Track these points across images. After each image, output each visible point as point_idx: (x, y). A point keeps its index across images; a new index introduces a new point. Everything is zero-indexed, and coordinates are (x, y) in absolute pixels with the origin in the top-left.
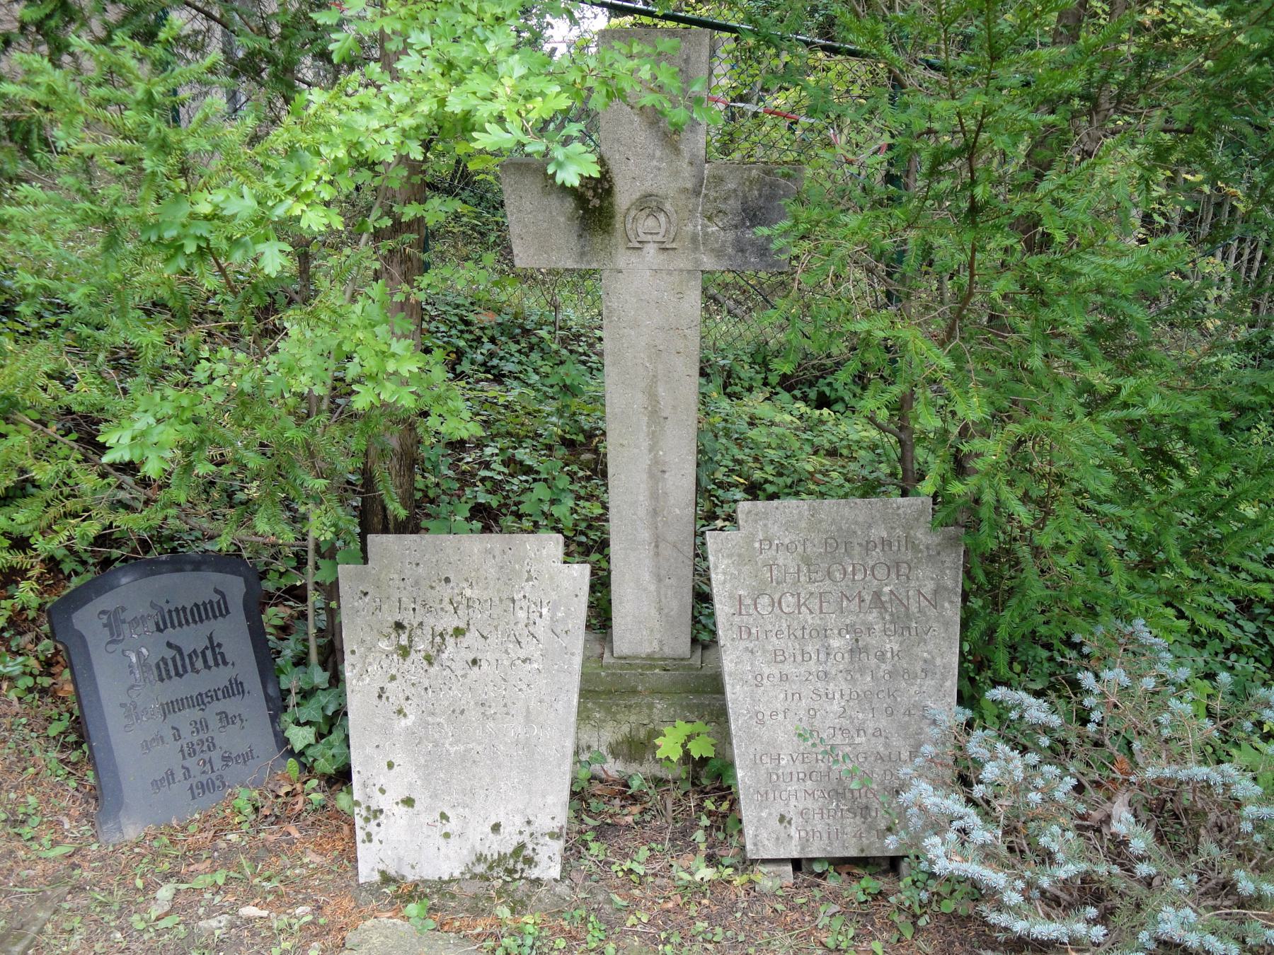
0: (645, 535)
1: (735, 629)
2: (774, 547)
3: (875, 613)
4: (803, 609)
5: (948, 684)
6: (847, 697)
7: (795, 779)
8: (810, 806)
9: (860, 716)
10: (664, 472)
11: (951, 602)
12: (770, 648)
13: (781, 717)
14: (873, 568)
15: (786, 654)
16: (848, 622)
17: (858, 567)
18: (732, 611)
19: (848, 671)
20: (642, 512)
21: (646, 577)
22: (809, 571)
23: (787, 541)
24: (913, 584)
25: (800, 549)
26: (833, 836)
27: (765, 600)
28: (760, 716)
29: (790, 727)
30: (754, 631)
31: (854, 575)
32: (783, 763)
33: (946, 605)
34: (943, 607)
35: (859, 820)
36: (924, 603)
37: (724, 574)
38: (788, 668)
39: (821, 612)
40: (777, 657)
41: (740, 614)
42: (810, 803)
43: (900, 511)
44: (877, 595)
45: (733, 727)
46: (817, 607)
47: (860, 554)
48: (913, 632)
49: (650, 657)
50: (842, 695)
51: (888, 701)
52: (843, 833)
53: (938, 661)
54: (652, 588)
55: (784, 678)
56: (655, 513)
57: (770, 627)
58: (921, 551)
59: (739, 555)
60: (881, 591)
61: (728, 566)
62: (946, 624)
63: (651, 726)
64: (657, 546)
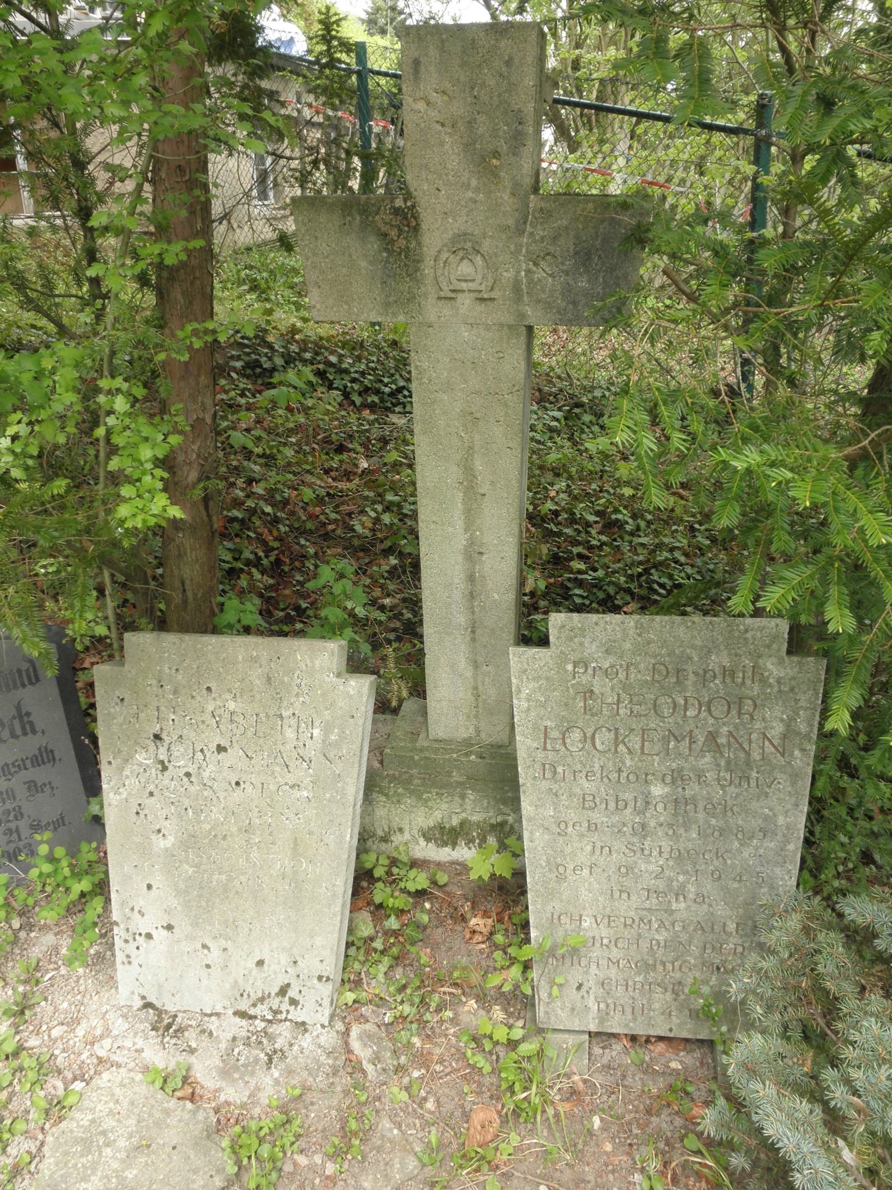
0: (461, 619)
1: (538, 766)
2: (590, 671)
3: (708, 758)
4: (621, 747)
5: (791, 847)
6: (665, 855)
7: (598, 945)
8: (613, 976)
9: (681, 878)
10: (481, 553)
11: (803, 750)
12: (578, 791)
13: (586, 871)
14: (709, 704)
15: (598, 800)
16: (674, 766)
17: (691, 701)
18: (535, 745)
19: (670, 826)
20: (457, 595)
21: (463, 664)
22: (631, 701)
23: (606, 665)
24: (758, 725)
25: (622, 676)
26: (638, 1011)
27: (576, 735)
28: (561, 869)
29: (596, 886)
30: (560, 770)
31: (686, 710)
32: (585, 925)
33: (797, 753)
34: (791, 755)
35: (669, 996)
36: (769, 749)
37: (528, 700)
38: (597, 817)
39: (643, 752)
40: (586, 802)
41: (545, 749)
42: (613, 972)
43: (749, 635)
44: (712, 737)
45: (528, 880)
46: (637, 747)
47: (695, 684)
48: (753, 783)
50: (660, 853)
51: (716, 863)
52: (650, 1009)
53: (781, 820)
54: (469, 674)
55: (593, 827)
56: (472, 596)
57: (578, 767)
58: (770, 686)
59: (547, 679)
60: (717, 732)
61: (534, 691)
62: (795, 777)
63: (464, 815)
64: (473, 632)
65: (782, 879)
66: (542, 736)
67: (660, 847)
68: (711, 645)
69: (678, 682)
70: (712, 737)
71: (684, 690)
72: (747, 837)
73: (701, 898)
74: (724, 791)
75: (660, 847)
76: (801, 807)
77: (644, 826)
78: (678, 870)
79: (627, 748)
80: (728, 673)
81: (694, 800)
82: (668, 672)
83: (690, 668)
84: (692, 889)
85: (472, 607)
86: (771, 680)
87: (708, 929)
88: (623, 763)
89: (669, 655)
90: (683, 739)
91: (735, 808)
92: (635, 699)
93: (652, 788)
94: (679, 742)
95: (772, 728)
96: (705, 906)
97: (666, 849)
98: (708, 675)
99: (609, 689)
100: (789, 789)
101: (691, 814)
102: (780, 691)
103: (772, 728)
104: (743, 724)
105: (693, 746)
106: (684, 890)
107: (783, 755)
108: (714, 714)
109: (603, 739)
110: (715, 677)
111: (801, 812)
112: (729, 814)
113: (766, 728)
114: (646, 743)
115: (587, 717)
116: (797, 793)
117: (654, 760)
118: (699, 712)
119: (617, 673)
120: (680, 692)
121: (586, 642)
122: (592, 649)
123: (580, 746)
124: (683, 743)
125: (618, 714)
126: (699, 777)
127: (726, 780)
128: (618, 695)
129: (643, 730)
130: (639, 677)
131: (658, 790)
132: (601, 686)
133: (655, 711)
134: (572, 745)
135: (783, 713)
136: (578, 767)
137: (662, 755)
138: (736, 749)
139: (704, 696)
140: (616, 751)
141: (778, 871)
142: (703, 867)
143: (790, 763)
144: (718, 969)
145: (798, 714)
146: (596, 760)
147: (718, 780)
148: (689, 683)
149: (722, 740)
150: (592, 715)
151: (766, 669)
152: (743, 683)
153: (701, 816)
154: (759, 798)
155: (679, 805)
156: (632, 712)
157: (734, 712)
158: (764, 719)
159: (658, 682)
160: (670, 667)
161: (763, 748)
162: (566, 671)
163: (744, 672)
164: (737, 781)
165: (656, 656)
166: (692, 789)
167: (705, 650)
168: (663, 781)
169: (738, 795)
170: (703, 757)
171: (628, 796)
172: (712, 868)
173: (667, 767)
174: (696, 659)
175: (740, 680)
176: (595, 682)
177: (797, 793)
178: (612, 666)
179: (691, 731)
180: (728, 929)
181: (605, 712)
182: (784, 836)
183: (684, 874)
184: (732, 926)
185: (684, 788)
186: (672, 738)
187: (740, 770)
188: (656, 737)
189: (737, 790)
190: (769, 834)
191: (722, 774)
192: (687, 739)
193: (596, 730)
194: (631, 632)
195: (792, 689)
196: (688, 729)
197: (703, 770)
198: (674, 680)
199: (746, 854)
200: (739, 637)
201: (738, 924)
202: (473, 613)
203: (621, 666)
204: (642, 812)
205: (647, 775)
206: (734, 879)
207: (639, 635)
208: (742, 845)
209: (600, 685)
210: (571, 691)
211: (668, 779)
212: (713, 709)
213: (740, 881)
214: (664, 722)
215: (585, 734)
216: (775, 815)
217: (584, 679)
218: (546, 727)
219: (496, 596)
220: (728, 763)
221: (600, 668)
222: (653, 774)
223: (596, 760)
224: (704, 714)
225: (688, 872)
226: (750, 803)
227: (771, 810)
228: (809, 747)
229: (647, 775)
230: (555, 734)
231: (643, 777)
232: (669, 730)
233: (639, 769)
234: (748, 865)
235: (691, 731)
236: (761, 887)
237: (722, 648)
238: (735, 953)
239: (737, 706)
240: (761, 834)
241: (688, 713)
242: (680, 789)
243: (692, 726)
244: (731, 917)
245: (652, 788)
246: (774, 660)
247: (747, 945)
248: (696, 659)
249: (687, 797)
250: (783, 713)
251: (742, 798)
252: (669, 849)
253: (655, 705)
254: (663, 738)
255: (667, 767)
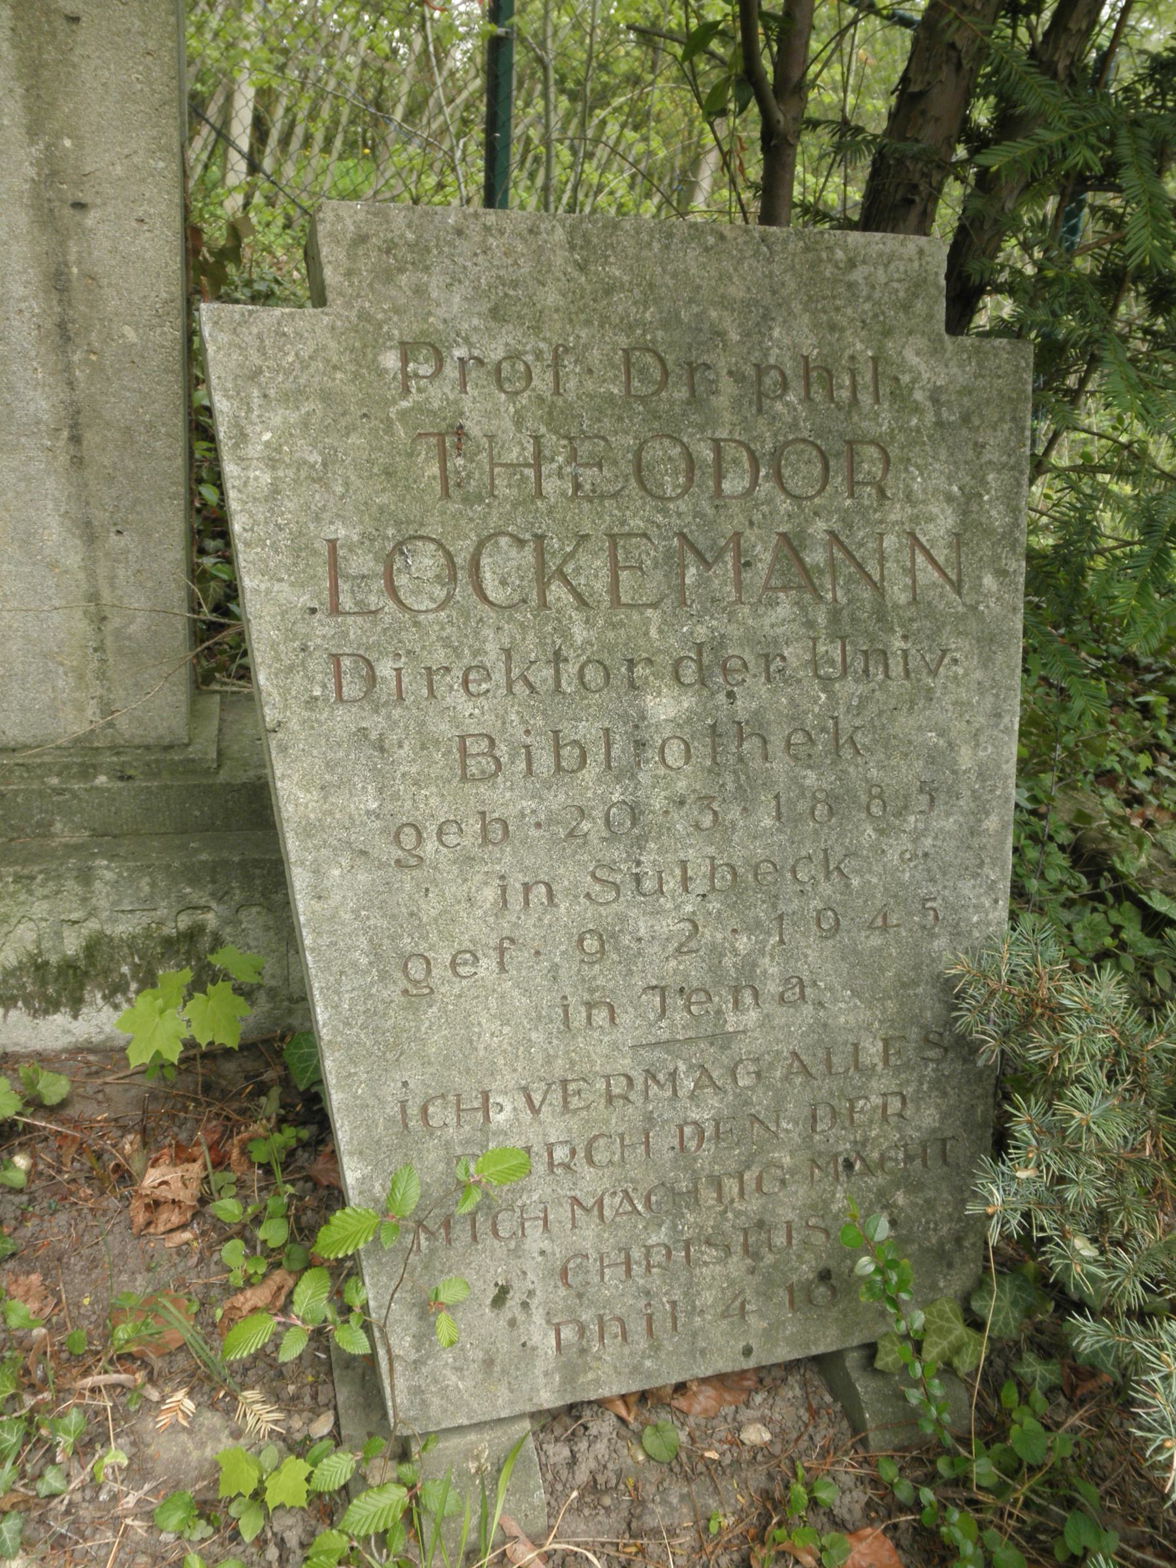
0: (40, 403)
1: (318, 665)
2: (451, 371)
3: (784, 609)
4: (557, 592)
5: (991, 823)
6: (699, 886)
7: (541, 1168)
8: (588, 1246)
9: (743, 943)
10: (79, 206)
11: (1001, 573)
12: (443, 728)
13: (487, 965)
14: (777, 455)
15: (502, 750)
16: (702, 632)
17: (730, 451)
18: (305, 600)
19: (705, 801)
20: (23, 333)
21: (54, 532)
22: (573, 457)
23: (495, 352)
24: (897, 513)
25: (542, 382)
26: (662, 1323)
27: (426, 561)
28: (416, 969)
29: (520, 1001)
30: (385, 669)
31: (719, 476)
32: (499, 1118)
33: (989, 581)
34: (977, 587)
35: (737, 1265)
36: (927, 575)
37: (272, 463)
38: (507, 798)
39: (616, 601)
40: (473, 758)
41: (335, 609)
42: (588, 1236)
43: (858, 275)
44: (791, 546)
45: (321, 1014)
46: (600, 585)
47: (737, 404)
48: (896, 669)
49: (83, 744)
50: (685, 880)
51: (825, 888)
52: (693, 1311)
53: (966, 758)
54: (73, 559)
55: (495, 831)
56: (64, 334)
57: (440, 656)
58: (917, 409)
59: (326, 396)
60: (802, 534)
61: (286, 434)
62: (988, 641)
63: (93, 925)
64: (76, 439)
65: (978, 908)
66: (323, 571)
67: (683, 864)
68: (768, 299)
69: (695, 400)
70: (791, 546)
71: (711, 421)
72: (890, 808)
73: (796, 991)
74: (831, 695)
75: (683, 864)
76: (1006, 720)
77: (635, 811)
78: (734, 923)
79: (573, 590)
80: (817, 374)
81: (757, 728)
82: (666, 373)
83: (723, 363)
84: (770, 967)
85: (68, 368)
86: (918, 395)
87: (817, 1069)
88: (566, 635)
89: (665, 325)
90: (719, 557)
91: (859, 737)
92: (584, 449)
93: (650, 701)
94: (708, 566)
95: (931, 519)
96: (808, 1009)
97: (699, 870)
98: (768, 381)
99: (508, 424)
100: (978, 675)
101: (756, 764)
102: (939, 424)
103: (931, 519)
104: (862, 511)
105: (747, 576)
106: (752, 975)
107: (958, 587)
108: (790, 485)
109: (505, 568)
110: (785, 386)
111: (1007, 731)
112: (847, 753)
113: (915, 519)
114: (624, 575)
115: (454, 507)
116: (995, 684)
117: (647, 622)
118: (755, 482)
119: (529, 378)
120: (702, 429)
121: (435, 284)
122: (452, 306)
123: (440, 593)
124: (718, 569)
125: (539, 493)
126: (767, 659)
127: (832, 663)
128: (537, 439)
129: (612, 537)
130: (590, 385)
131: (665, 706)
132: (487, 414)
133: (641, 482)
134: (416, 592)
135: (950, 479)
136: (440, 656)
137: (667, 605)
138: (850, 579)
139: (760, 438)
140: (544, 604)
141: (967, 887)
142: (795, 905)
143: (974, 608)
144: (849, 1165)
145: (983, 482)
146: (488, 632)
147: (815, 664)
148: (722, 401)
149: (815, 557)
150: (466, 500)
151: (903, 366)
152: (854, 401)
153: (780, 765)
154: (913, 703)
155: (722, 739)
156: (577, 486)
157: (838, 480)
158: (909, 497)
159: (643, 399)
160: (670, 359)
161: (912, 572)
162: (381, 373)
163: (853, 374)
164: (859, 665)
165: (631, 328)
166: (754, 696)
167: (756, 314)
168: (677, 678)
169: (864, 701)
170: (773, 603)
171: (587, 730)
172: (816, 903)
173: (684, 639)
174: (734, 336)
175: (845, 394)
176: (467, 404)
177: (995, 684)
178: (513, 356)
179: (738, 535)
180: (865, 1060)
181: (502, 490)
182: (975, 796)
183: (749, 931)
184: (873, 1050)
185: (731, 695)
186: (690, 557)
187: (864, 634)
188: (649, 553)
189: (861, 689)
190: (943, 796)
191: (821, 649)
192: (729, 558)
193: (481, 545)
194: (559, 259)
195: (966, 418)
196: (729, 529)
197: (775, 641)
198: (682, 393)
199: (893, 856)
200: (835, 281)
201: (886, 1042)
202: (71, 384)
203: (539, 355)
204: (629, 773)
205: (631, 664)
206: (871, 927)
207: (582, 268)
208: (881, 832)
209: (482, 410)
210: (400, 430)
211: (689, 673)
212: (787, 472)
213: (885, 928)
214: (664, 511)
215: (449, 556)
216: (950, 744)
217: (439, 394)
218: (332, 543)
219: (131, 334)
220: (835, 616)
221: (480, 362)
222: (649, 661)
223: (488, 632)
224: (766, 487)
225: (758, 924)
226: (892, 720)
227: (941, 735)
228: (1012, 566)
229: (631, 664)
230: (361, 563)
231: (625, 673)
232: (682, 536)
233: (611, 648)
234: (901, 885)
235: (738, 535)
236: (933, 936)
237: (797, 307)
238: (885, 1118)
239: (844, 462)
240: (924, 799)
241: (726, 485)
242: (721, 698)
243: (739, 521)
244: (868, 1028)
245: (650, 701)
246: (920, 342)
247: (909, 1090)
248: (734, 336)
249: (742, 716)
250: (950, 479)
251: (872, 709)
252: (705, 869)
253: (638, 469)
254: (669, 554)
255: (684, 639)
